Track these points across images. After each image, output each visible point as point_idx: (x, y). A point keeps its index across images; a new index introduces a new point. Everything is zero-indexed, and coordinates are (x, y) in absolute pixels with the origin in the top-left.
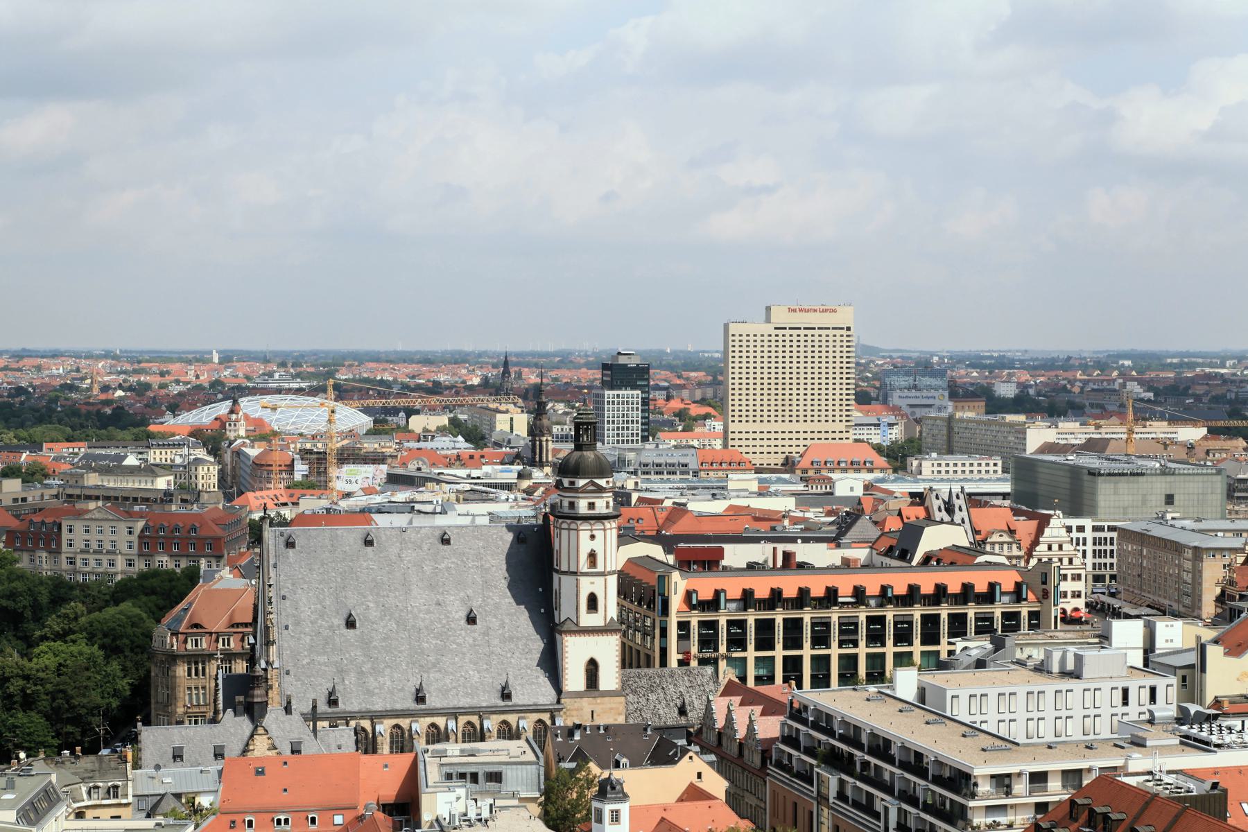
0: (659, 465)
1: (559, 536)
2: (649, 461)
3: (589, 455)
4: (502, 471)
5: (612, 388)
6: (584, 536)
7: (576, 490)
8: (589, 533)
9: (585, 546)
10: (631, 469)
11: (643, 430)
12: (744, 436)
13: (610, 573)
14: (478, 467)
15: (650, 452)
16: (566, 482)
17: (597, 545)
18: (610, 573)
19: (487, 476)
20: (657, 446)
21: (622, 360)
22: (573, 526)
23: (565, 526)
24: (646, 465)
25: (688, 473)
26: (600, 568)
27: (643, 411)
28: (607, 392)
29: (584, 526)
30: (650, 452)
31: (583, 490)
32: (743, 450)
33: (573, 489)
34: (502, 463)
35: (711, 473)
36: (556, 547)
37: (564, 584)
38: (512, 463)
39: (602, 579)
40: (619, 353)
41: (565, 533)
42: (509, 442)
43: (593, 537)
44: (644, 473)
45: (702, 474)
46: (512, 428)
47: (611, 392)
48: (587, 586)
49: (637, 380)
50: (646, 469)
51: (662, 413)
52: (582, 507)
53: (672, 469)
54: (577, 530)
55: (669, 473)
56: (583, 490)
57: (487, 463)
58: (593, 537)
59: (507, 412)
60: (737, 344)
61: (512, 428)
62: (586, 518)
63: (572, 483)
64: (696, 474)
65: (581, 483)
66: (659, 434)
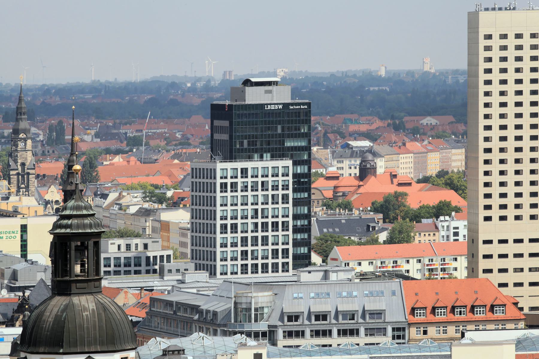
0: (322, 317)
2: (301, 307)
5: (230, 157)
10: (262, 326)
11: (296, 244)
12: (511, 249)
15: (307, 291)
20: (326, 276)
21: (254, 97)
24: (293, 317)
25: (382, 331)
27: (297, 203)
28: (220, 166)
30: (307, 291)
32: (510, 278)
35: (432, 331)
40: (247, 83)
42: (14, 276)
44: (289, 334)
45: (413, 332)
46: (24, 247)
47: (229, 165)
49: (283, 137)
50: (293, 326)
51: (348, 206)
53: (349, 324)
55: (343, 333)
59: (14, 213)
60: (496, 54)
61: (24, 247)
64: (399, 333)
66: (337, 251)
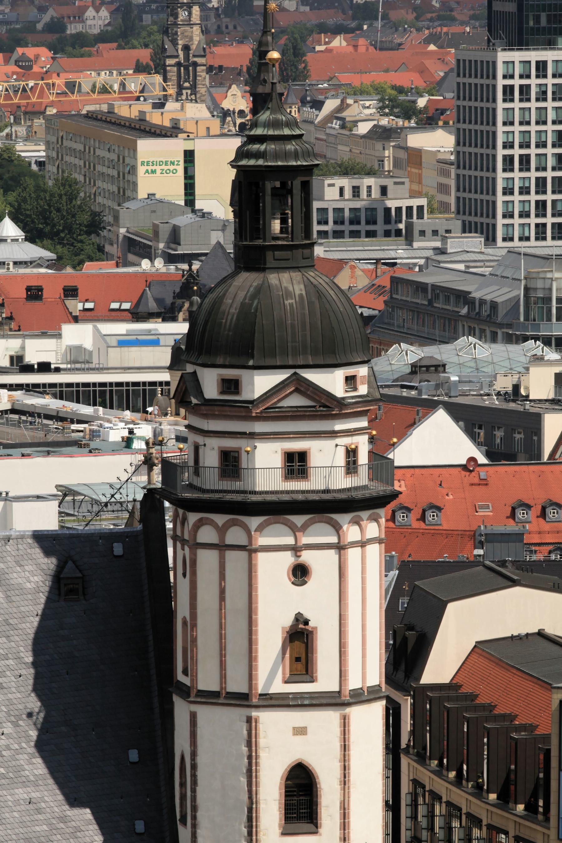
1: (191, 568)
3: (289, 284)
4: (124, 343)
6: (272, 569)
7: (245, 410)
8: (287, 560)
9: (276, 602)
13: (360, 697)
14: (51, 331)
16: (210, 382)
17: (315, 602)
18: (360, 697)
19: (78, 358)
22: (235, 536)
23: (207, 535)
26: (326, 680)
29: (275, 535)
31: (268, 409)
33: (232, 405)
34: (137, 315)
36: (182, 609)
37: (206, 737)
38: (169, 315)
39: (330, 718)
41: (207, 560)
43: (300, 573)
48: (281, 741)
52: (265, 466)
54: (250, 550)
56: (268, 409)
57: (87, 316)
58: (300, 573)
62: (277, 509)
63: (231, 386)
65: (261, 383)
